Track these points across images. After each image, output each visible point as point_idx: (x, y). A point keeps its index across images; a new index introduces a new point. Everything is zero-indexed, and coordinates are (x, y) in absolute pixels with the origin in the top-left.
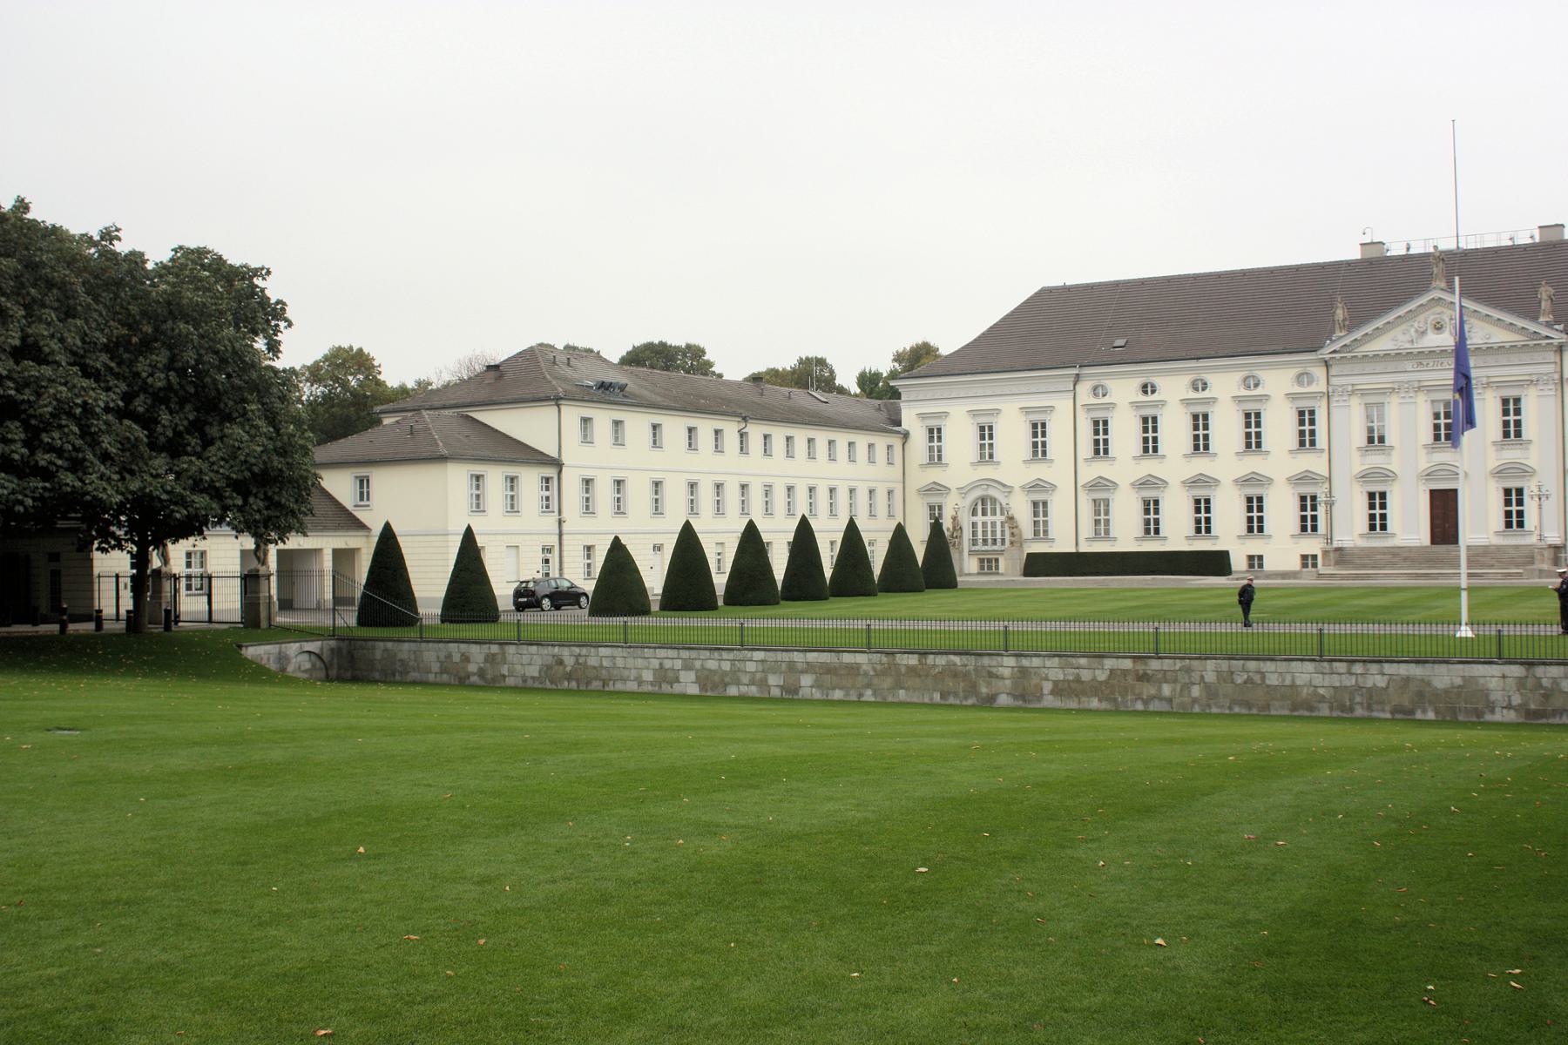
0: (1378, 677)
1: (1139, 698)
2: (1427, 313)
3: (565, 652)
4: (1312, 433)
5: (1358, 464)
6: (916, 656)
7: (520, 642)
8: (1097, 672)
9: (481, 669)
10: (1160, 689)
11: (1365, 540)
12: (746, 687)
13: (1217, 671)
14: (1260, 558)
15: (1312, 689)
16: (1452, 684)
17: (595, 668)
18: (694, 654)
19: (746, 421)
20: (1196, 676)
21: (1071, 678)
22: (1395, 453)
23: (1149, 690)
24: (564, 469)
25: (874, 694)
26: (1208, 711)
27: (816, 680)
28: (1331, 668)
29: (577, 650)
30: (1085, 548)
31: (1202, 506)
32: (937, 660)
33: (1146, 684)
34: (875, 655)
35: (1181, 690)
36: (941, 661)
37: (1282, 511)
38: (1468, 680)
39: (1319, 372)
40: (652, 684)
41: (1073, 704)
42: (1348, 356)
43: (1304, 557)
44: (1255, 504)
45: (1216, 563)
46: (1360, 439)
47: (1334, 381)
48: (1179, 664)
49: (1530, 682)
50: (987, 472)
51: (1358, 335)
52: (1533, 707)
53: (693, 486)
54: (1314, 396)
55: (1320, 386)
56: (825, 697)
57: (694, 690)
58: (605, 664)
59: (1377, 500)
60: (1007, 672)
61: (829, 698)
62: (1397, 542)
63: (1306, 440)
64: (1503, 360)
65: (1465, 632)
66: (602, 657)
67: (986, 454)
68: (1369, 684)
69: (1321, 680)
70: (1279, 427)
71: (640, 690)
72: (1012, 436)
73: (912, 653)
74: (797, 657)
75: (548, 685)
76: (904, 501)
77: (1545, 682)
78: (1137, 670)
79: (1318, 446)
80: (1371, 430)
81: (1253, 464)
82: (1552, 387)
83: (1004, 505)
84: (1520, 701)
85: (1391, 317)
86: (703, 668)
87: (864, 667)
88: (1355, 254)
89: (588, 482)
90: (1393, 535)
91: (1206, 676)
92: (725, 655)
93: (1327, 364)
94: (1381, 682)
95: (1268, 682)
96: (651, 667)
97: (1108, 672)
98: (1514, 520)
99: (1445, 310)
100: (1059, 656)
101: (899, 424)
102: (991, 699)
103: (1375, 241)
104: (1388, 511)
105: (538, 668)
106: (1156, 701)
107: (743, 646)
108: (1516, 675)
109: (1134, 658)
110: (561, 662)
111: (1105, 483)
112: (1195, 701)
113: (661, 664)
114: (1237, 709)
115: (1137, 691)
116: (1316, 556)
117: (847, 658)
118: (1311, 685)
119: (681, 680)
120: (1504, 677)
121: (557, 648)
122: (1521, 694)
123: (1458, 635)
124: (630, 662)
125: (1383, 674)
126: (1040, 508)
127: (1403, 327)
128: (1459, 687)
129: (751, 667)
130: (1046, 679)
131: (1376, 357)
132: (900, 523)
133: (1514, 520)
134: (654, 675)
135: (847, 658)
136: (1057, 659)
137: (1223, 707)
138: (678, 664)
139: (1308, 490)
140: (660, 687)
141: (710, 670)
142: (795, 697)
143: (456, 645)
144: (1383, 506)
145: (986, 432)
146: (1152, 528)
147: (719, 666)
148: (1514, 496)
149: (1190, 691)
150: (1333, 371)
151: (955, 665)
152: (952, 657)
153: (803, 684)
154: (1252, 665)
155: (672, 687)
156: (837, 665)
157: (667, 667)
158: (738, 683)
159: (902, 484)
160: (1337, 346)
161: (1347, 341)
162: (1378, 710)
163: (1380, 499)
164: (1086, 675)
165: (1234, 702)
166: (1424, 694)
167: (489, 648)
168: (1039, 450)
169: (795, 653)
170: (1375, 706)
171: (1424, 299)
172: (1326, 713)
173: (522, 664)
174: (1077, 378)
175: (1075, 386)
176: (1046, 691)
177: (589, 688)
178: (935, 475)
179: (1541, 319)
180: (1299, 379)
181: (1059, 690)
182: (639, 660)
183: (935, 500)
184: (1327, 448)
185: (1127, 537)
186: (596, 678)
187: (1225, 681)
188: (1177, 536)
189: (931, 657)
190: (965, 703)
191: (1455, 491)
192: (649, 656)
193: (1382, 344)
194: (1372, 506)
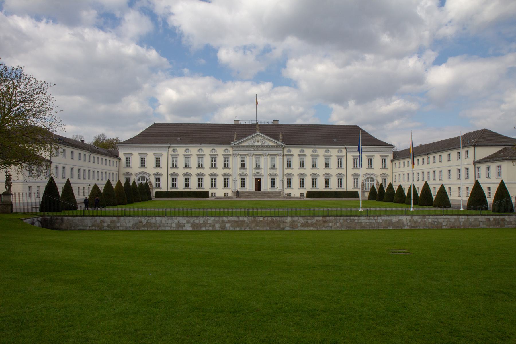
0: (380, 220)
1: (324, 227)
2: (255, 138)
3: (143, 219)
4: (228, 164)
5: (239, 172)
6: (262, 218)
7: (125, 216)
8: (313, 221)
9: (109, 225)
10: (329, 224)
11: (240, 190)
12: (208, 228)
13: (343, 220)
14: (215, 193)
15: (365, 223)
16: (396, 221)
17: (154, 223)
18: (190, 218)
19: (91, 152)
21: (306, 222)
22: (247, 169)
23: (327, 225)
24: (52, 164)
25: (249, 228)
26: (341, 229)
27: (231, 225)
29: (148, 218)
30: (169, 190)
31: (200, 180)
32: (268, 219)
34: (250, 218)
35: (334, 224)
36: (270, 219)
37: (220, 182)
38: (399, 220)
39: (230, 150)
40: (175, 228)
41: (306, 229)
43: (225, 193)
44: (213, 180)
45: (205, 194)
46: (239, 166)
47: (233, 152)
48: (334, 218)
49: (412, 220)
50: (143, 170)
51: (240, 141)
52: (412, 225)
53: (79, 170)
54: (229, 155)
55: (230, 153)
56: (234, 230)
57: (190, 229)
58: (158, 222)
59: (243, 180)
60: (288, 221)
61: (235, 230)
62: (247, 190)
63: (226, 165)
65: (361, 210)
66: (157, 220)
67: (143, 164)
68: (378, 222)
70: (220, 162)
71: (171, 229)
72: (150, 160)
73: (262, 217)
74: (225, 219)
75: (136, 229)
76: (119, 177)
77: (415, 220)
78: (323, 220)
79: (229, 167)
80: (199, 163)
81: (213, 171)
82: (282, 156)
83: (148, 178)
84: (410, 224)
85: (248, 138)
86: (193, 222)
87: (246, 221)
88: (233, 123)
89: (57, 167)
90: (247, 189)
91: (340, 221)
92: (201, 218)
93: (232, 147)
94: (381, 221)
95: (355, 222)
96: (175, 222)
97: (315, 221)
98: (273, 186)
99: (260, 138)
100: (303, 217)
101: (118, 156)
102: (283, 228)
103: (238, 120)
104: (245, 183)
105: (132, 224)
106: (328, 227)
107: (207, 216)
108: (409, 218)
109: (323, 217)
110: (141, 222)
111: (189, 174)
112: (337, 227)
113: (179, 222)
114: (348, 229)
116: (228, 193)
117: (241, 219)
118: (365, 222)
119: (186, 226)
120: (407, 219)
121: (140, 218)
122: (410, 223)
123: (360, 210)
124: (167, 221)
126: (158, 180)
127: (250, 140)
128: (398, 222)
129: (210, 222)
130: (299, 223)
131: (244, 147)
132: (390, 183)
133: (273, 186)
134: (176, 225)
135: (241, 219)
137: (344, 228)
138: (185, 222)
139: (226, 177)
140: (178, 228)
141: (196, 223)
142: (224, 230)
143: (99, 217)
144: (244, 182)
145: (143, 160)
146: (187, 185)
147: (199, 222)
148: (273, 180)
149: (336, 224)
150: (233, 150)
151: (273, 219)
152: (273, 218)
153: (227, 226)
154: (352, 218)
155: (182, 228)
156: (238, 221)
157: (181, 222)
158: (205, 226)
159: (118, 172)
160: (235, 144)
161: (238, 143)
162: (380, 228)
163: (214, 180)
164: (310, 221)
166: (391, 223)
167: (113, 218)
168: (158, 165)
169: (225, 218)
170: (379, 227)
171: (255, 134)
172: (368, 229)
173: (125, 223)
174: (169, 147)
175: (168, 149)
176: (299, 226)
177: (152, 229)
178: (128, 170)
179: (280, 141)
180: (225, 151)
181: (302, 225)
182: (171, 220)
183: (128, 177)
184: (231, 167)
185: (181, 187)
186: (155, 227)
188: (194, 187)
189: (267, 218)
190: (276, 230)
191: (260, 179)
192: (175, 219)
193: (245, 144)
194: (241, 182)
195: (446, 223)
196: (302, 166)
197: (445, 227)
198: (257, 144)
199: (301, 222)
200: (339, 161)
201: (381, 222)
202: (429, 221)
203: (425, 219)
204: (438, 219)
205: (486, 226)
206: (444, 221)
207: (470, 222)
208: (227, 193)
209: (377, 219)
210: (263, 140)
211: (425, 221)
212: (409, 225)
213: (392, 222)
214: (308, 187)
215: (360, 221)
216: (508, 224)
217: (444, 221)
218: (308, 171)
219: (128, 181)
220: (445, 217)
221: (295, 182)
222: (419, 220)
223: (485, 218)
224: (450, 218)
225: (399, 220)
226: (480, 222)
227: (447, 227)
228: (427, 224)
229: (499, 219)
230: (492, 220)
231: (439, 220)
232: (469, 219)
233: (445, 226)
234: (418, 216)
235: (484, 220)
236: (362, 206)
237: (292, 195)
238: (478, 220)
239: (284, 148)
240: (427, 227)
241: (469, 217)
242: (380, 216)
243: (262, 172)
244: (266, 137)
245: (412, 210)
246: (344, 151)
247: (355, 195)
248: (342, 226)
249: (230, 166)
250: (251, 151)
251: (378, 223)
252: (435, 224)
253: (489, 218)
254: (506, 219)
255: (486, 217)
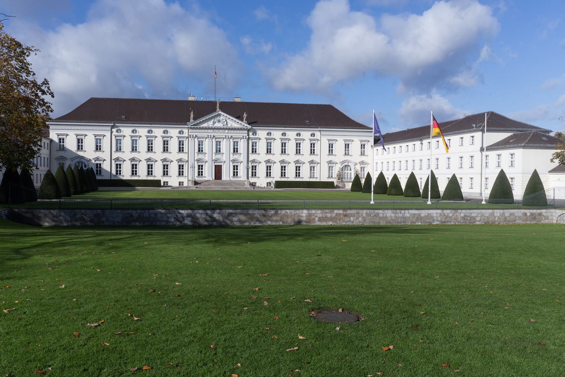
0: (408, 214)
1: (344, 221)
10: (350, 219)
14: (167, 182)
15: (391, 217)
20: (360, 214)
23: (347, 219)
28: (396, 212)
31: (150, 167)
33: (346, 217)
35: (356, 219)
37: (173, 169)
39: (186, 131)
41: (324, 224)
42: (195, 127)
43: (180, 182)
44: (165, 167)
48: (355, 211)
52: (443, 220)
54: (183, 137)
59: (200, 167)
60: (304, 215)
62: (206, 179)
63: (181, 150)
64: (235, 131)
68: (405, 216)
69: (393, 215)
70: (173, 145)
77: (446, 214)
81: (166, 155)
84: (440, 219)
94: (408, 215)
95: (380, 216)
97: (335, 214)
112: (360, 222)
114: (371, 224)
115: (343, 220)
116: (183, 182)
118: (391, 217)
120: (437, 213)
125: (409, 213)
128: (427, 216)
130: (317, 217)
131: (203, 128)
133: (235, 174)
136: (320, 211)
148: (235, 168)
151: (287, 213)
154: (376, 211)
162: (407, 223)
164: (329, 215)
165: (370, 222)
170: (407, 222)
179: (244, 121)
181: (320, 220)
187: (368, 216)
195: (480, 218)
196: (269, 151)
197: (478, 222)
198: (217, 125)
199: (318, 216)
200: (312, 145)
201: (409, 217)
202: (461, 216)
203: (458, 214)
204: (471, 213)
205: (522, 222)
206: (477, 216)
207: (506, 217)
208: (182, 182)
209: (404, 213)
210: (225, 120)
211: (457, 215)
212: (439, 220)
213: (421, 216)
214: (276, 176)
215: (385, 215)
216: (545, 219)
217: (477, 216)
218: (277, 156)
219: (62, 167)
220: (479, 211)
221: (261, 170)
222: (451, 215)
223: (522, 212)
224: (484, 212)
225: (428, 214)
226: (516, 217)
227: (480, 222)
228: (459, 219)
229: (536, 214)
230: (528, 214)
231: (473, 215)
232: (504, 213)
233: (478, 221)
234: (450, 209)
235: (520, 215)
236: (373, 199)
237: (257, 185)
238: (514, 214)
239: (249, 130)
240: (459, 222)
241: (505, 211)
242: (408, 209)
243: (224, 158)
244: (228, 116)
245: (429, 203)
246: (318, 134)
247: (330, 185)
248: (365, 221)
249: (186, 150)
250: (211, 133)
251: (406, 217)
252: (467, 219)
253: (525, 212)
254: (544, 214)
255: (523, 211)
